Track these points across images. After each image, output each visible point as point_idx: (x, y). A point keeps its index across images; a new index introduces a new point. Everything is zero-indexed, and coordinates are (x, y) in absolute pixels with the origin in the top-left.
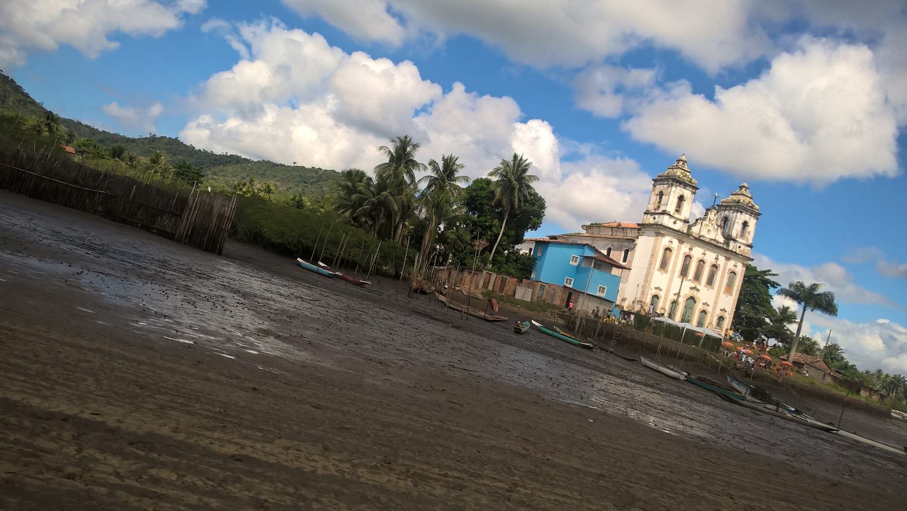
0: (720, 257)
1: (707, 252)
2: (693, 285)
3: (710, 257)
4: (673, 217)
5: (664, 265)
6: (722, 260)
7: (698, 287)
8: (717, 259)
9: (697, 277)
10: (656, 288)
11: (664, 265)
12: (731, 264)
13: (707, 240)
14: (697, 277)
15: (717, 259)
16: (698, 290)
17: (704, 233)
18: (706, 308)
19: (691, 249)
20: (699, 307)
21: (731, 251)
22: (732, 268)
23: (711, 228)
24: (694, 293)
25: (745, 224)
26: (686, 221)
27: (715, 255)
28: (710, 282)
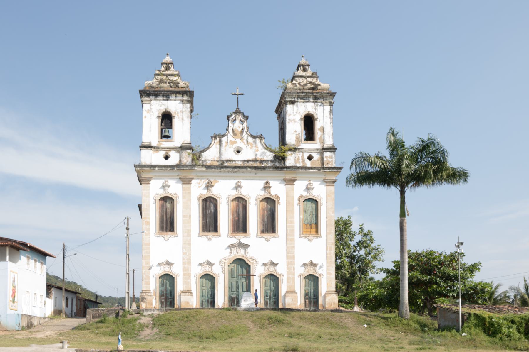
0: (272, 183)
1: (243, 183)
2: (234, 241)
3: (253, 189)
4: (163, 149)
5: (167, 224)
6: (278, 188)
7: (244, 241)
8: (267, 187)
9: (240, 225)
10: (160, 264)
11: (167, 224)
12: (300, 187)
13: (240, 164)
14: (240, 225)
15: (267, 187)
16: (245, 246)
17: (229, 154)
18: (271, 270)
19: (209, 186)
20: (259, 272)
21: (295, 168)
22: (305, 194)
23: (239, 143)
24: (241, 253)
25: (309, 122)
26: (183, 148)
27: (261, 183)
28: (269, 225)
